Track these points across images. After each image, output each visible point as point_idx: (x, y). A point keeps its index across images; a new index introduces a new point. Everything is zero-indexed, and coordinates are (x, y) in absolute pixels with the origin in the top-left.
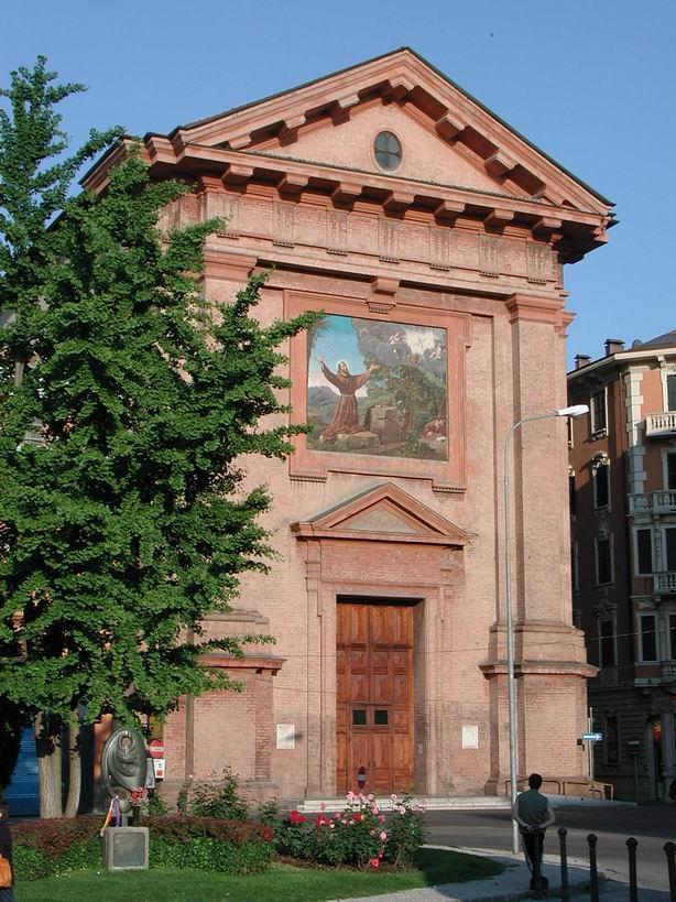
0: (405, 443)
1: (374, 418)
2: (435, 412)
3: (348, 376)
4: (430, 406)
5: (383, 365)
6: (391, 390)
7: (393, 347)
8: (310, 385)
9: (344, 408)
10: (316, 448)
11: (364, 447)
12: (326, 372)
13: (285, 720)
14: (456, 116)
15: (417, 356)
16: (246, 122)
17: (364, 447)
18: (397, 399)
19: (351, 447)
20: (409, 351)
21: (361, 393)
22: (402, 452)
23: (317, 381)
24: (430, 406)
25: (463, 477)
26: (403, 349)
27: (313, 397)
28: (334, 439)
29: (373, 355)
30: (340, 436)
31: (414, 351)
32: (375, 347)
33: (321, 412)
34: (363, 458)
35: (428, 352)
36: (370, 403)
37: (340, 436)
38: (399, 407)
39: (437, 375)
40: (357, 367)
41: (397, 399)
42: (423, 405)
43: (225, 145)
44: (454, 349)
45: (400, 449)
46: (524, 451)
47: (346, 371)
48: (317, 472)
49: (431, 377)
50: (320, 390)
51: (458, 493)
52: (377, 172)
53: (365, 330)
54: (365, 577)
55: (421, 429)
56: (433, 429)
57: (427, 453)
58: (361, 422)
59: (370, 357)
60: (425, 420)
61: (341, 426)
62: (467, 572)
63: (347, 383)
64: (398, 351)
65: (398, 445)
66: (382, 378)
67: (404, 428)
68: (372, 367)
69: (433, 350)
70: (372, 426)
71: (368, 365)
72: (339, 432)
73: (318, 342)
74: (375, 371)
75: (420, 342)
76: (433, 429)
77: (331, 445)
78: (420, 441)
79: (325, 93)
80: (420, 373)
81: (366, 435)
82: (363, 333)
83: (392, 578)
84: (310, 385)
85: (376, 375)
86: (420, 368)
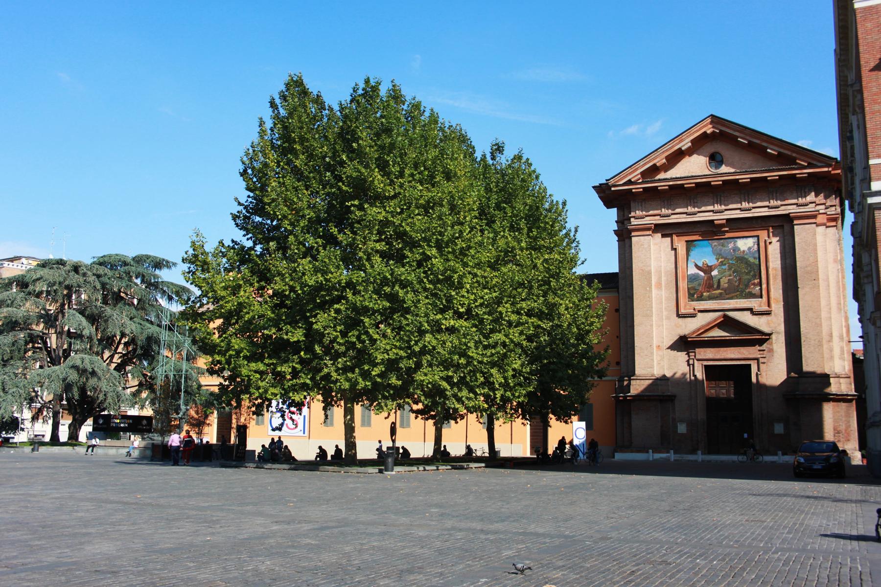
0: (738, 293)
2: (754, 277)
3: (708, 266)
4: (751, 274)
5: (726, 258)
6: (730, 269)
7: (730, 249)
8: (688, 273)
9: (706, 281)
10: (693, 301)
11: (717, 297)
12: (697, 266)
13: (682, 421)
14: (741, 138)
15: (744, 251)
16: (637, 169)
17: (717, 297)
18: (734, 273)
19: (710, 298)
20: (739, 249)
21: (715, 273)
22: (737, 297)
23: (692, 270)
24: (751, 274)
25: (769, 305)
26: (736, 249)
27: (690, 279)
28: (702, 295)
29: (720, 255)
30: (705, 294)
31: (742, 249)
32: (721, 250)
33: (695, 284)
35: (749, 248)
36: (719, 277)
37: (705, 294)
38: (735, 277)
39: (755, 258)
40: (711, 261)
41: (734, 273)
42: (747, 274)
43: (630, 180)
44: (762, 244)
45: (736, 296)
46: (799, 290)
47: (707, 264)
49: (752, 260)
50: (693, 275)
51: (768, 313)
52: (710, 173)
53: (715, 244)
54: (718, 357)
55: (747, 286)
56: (754, 284)
57: (751, 296)
58: (715, 286)
59: (719, 255)
60: (750, 280)
62: (775, 350)
63: (707, 269)
64: (733, 250)
65: (735, 294)
67: (738, 286)
68: (720, 260)
69: (753, 247)
70: (721, 287)
71: (718, 259)
72: (704, 292)
73: (692, 253)
74: (722, 262)
75: (745, 244)
76: (754, 284)
77: (701, 298)
78: (747, 291)
79: (673, 147)
80: (745, 258)
81: (719, 291)
82: (715, 245)
83: (733, 356)
84: (688, 273)
85: (722, 264)
86: (746, 256)
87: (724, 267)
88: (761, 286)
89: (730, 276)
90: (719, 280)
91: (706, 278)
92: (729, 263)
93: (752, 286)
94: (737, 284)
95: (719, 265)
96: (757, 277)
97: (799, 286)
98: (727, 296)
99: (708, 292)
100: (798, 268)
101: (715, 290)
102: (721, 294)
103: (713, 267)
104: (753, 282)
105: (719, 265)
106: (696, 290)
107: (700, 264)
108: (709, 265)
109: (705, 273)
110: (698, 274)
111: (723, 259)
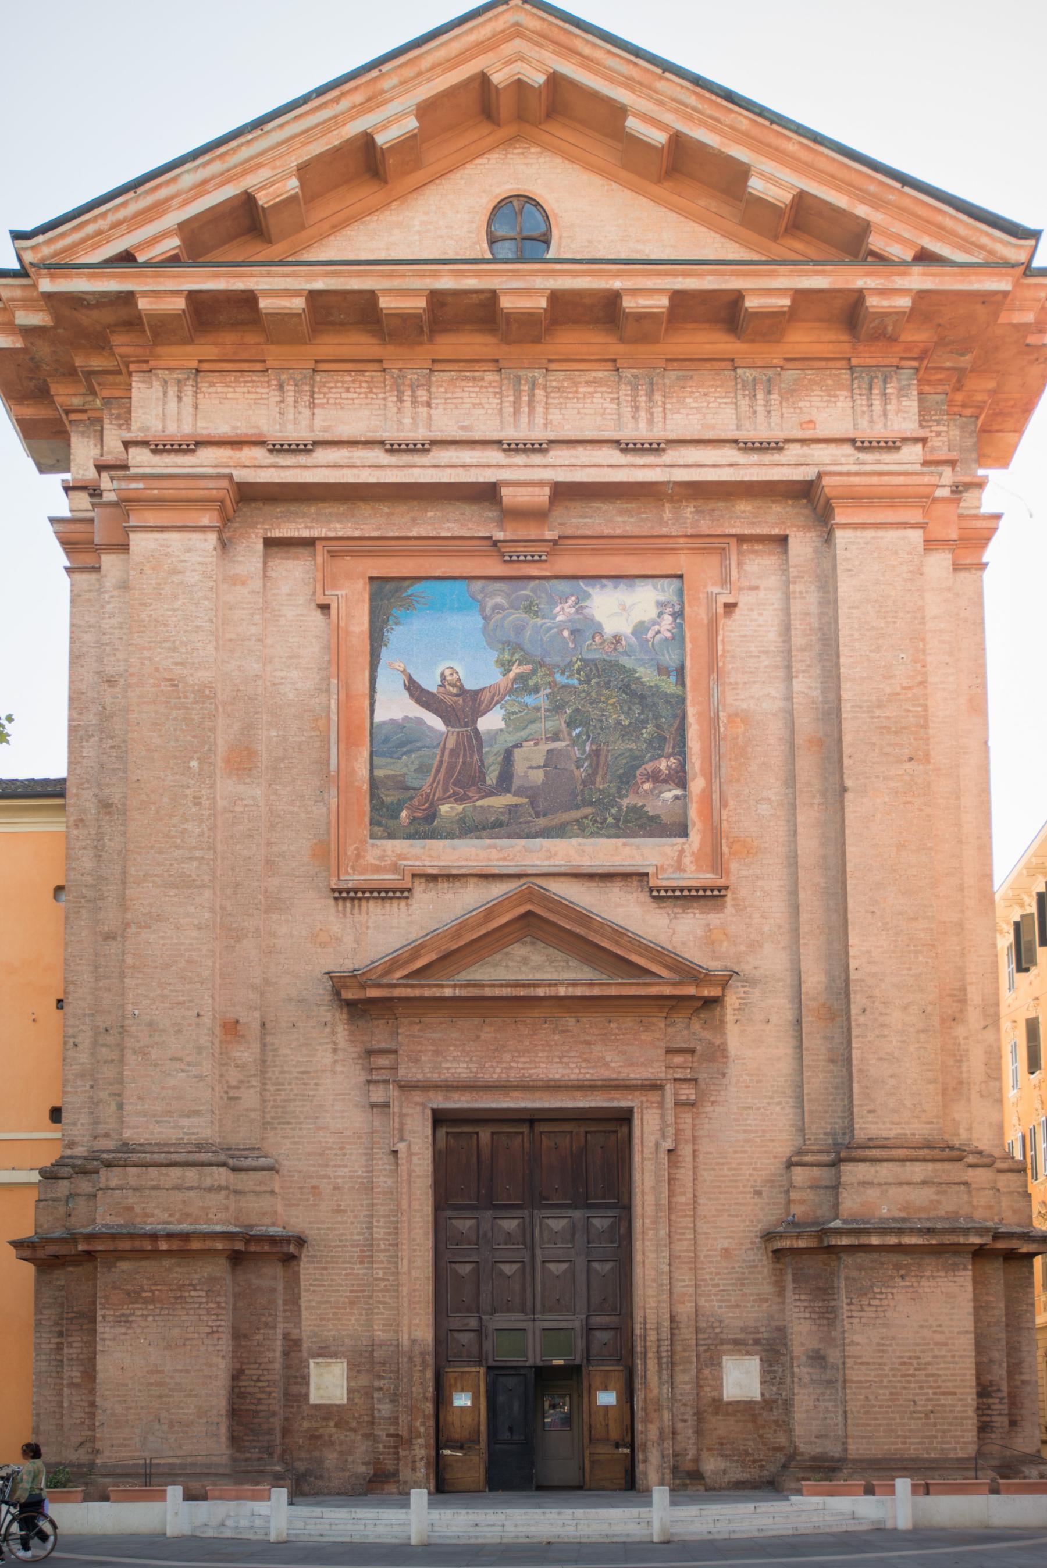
0: (589, 810)
1: (520, 767)
2: (657, 744)
6: (557, 708)
12: (413, 689)
15: (617, 639)
18: (571, 724)
21: (490, 722)
30: (444, 808)
31: (610, 628)
34: (495, 847)
35: (640, 629)
36: (510, 739)
42: (626, 733)
44: (697, 613)
48: (389, 878)
49: (648, 675)
55: (627, 780)
58: (492, 778)
61: (446, 790)
64: (573, 632)
66: (536, 690)
68: (516, 670)
70: (517, 783)
71: (505, 666)
76: (655, 777)
78: (625, 802)
87: (529, 700)
88: (683, 784)
89: (556, 737)
90: (508, 755)
91: (451, 743)
92: (552, 684)
93: (647, 786)
94: (582, 773)
95: (511, 692)
96: (668, 749)
97: (848, 783)
98: (542, 822)
99: (460, 800)
100: (846, 707)
101: (490, 794)
102: (512, 809)
103: (486, 697)
104: (649, 767)
105: (511, 692)
106: (408, 789)
107: (430, 683)
108: (468, 686)
109: (447, 722)
110: (419, 721)
111: (526, 668)
